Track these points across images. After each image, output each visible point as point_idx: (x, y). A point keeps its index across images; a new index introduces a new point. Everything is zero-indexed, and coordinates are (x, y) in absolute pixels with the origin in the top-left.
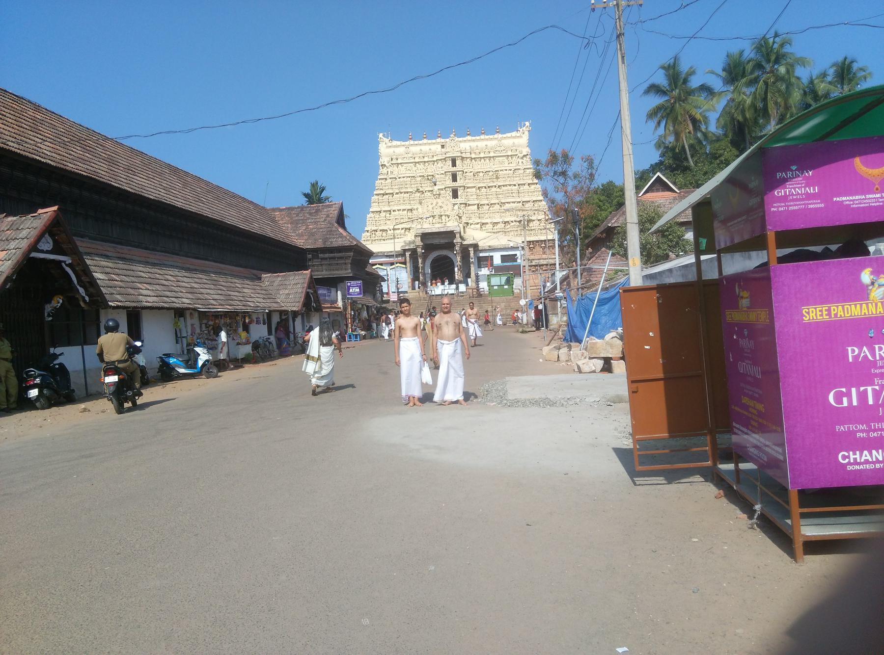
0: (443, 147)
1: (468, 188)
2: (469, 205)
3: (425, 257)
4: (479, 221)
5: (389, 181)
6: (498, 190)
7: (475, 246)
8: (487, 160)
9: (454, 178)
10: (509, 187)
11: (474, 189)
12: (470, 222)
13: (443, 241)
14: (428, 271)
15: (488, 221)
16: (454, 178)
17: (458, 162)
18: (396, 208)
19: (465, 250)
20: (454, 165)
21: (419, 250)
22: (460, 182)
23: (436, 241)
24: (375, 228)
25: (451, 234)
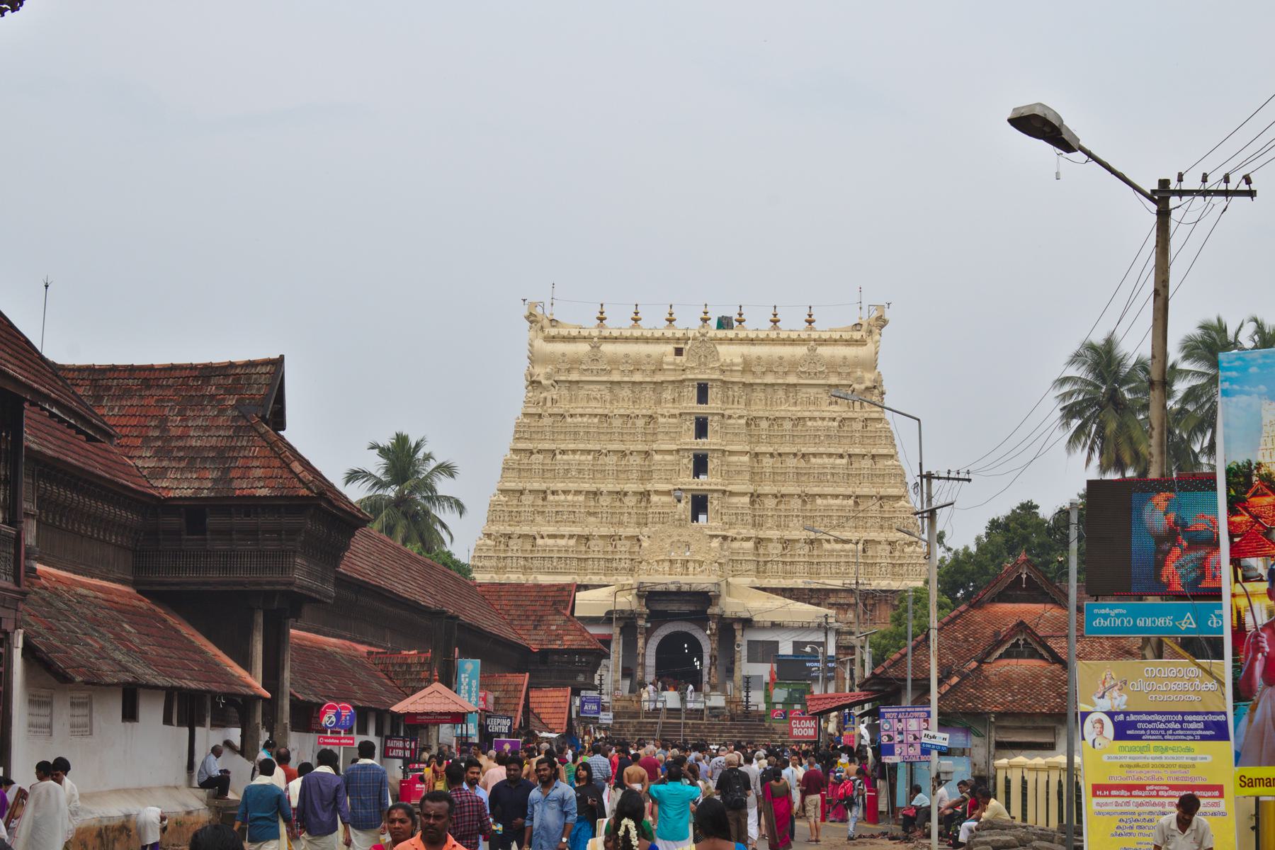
0: (679, 352)
1: (731, 453)
2: (732, 494)
3: (649, 633)
4: (753, 533)
5: (547, 421)
6: (802, 463)
7: (747, 623)
8: (781, 394)
9: (702, 428)
10: (826, 460)
11: (746, 459)
12: (731, 533)
13: (685, 608)
14: (651, 661)
15: (774, 534)
16: (702, 428)
17: (712, 393)
18: (560, 486)
19: (728, 628)
20: (703, 396)
21: (641, 622)
22: (710, 442)
23: (674, 607)
24: (508, 530)
25: (704, 599)
